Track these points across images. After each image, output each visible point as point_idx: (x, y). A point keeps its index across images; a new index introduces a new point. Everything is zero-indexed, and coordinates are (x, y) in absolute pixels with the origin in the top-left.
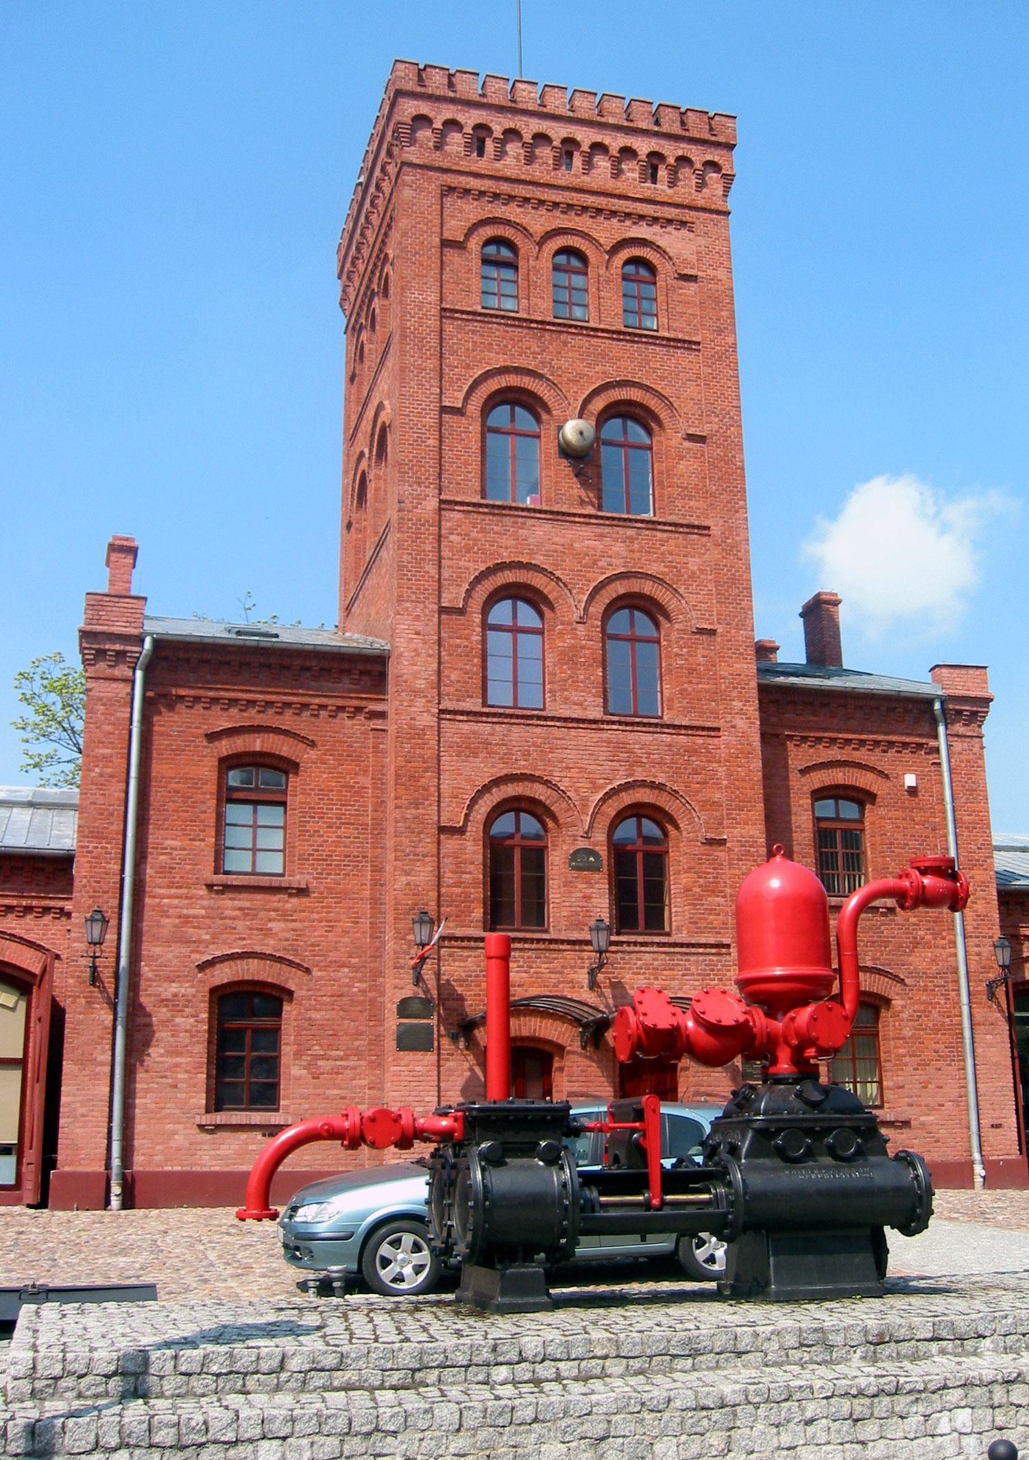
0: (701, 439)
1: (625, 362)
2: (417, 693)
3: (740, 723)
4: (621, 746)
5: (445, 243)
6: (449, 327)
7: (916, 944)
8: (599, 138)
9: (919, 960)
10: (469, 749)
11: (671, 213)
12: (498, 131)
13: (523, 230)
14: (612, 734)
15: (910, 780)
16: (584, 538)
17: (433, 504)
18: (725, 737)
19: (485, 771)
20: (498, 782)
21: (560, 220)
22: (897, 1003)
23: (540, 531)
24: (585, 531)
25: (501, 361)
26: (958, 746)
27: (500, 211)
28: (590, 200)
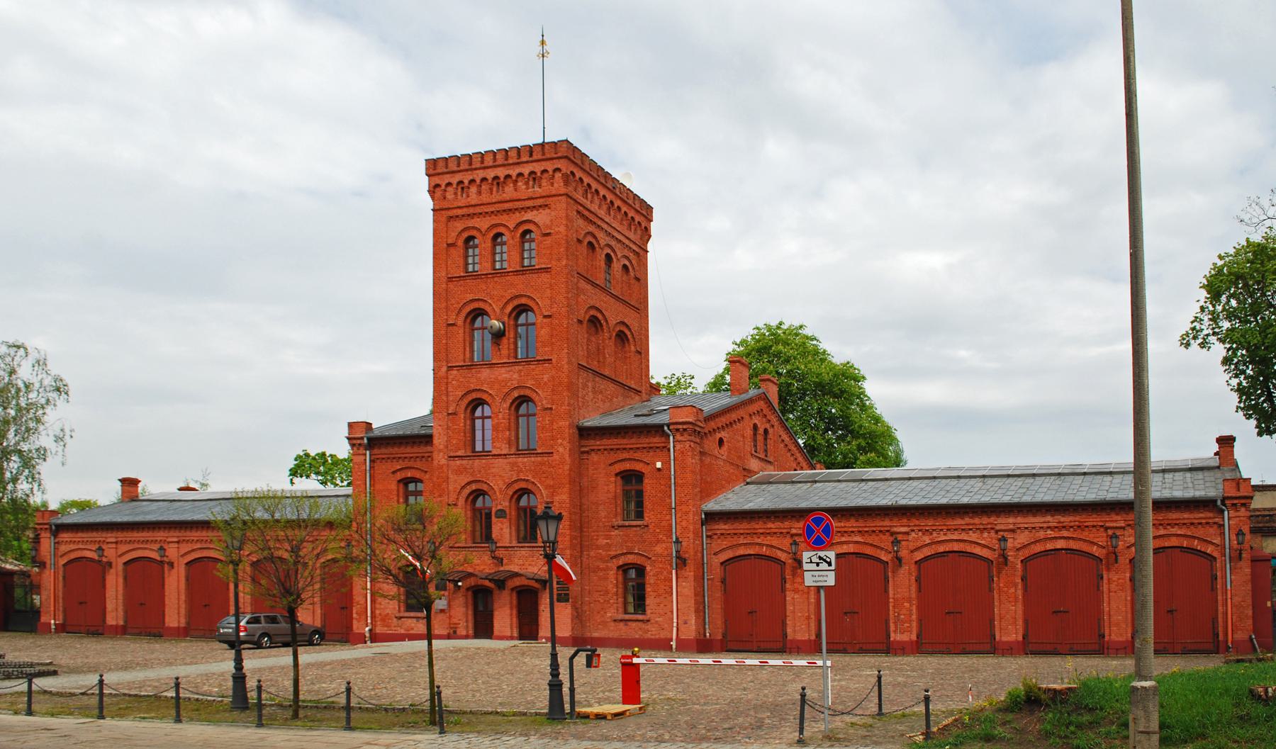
0: (549, 316)
1: (519, 285)
2: (440, 451)
3: (561, 449)
4: (515, 464)
5: (449, 245)
6: (451, 285)
7: (658, 541)
8: (507, 172)
9: (659, 549)
10: (459, 472)
11: (540, 202)
12: (466, 182)
13: (479, 230)
14: (512, 459)
15: (659, 465)
16: (503, 373)
17: (444, 369)
18: (556, 456)
19: (464, 479)
20: (469, 483)
21: (495, 220)
22: (648, 568)
23: (485, 373)
24: (503, 370)
25: (471, 297)
26: (678, 447)
27: (471, 223)
28: (507, 206)
